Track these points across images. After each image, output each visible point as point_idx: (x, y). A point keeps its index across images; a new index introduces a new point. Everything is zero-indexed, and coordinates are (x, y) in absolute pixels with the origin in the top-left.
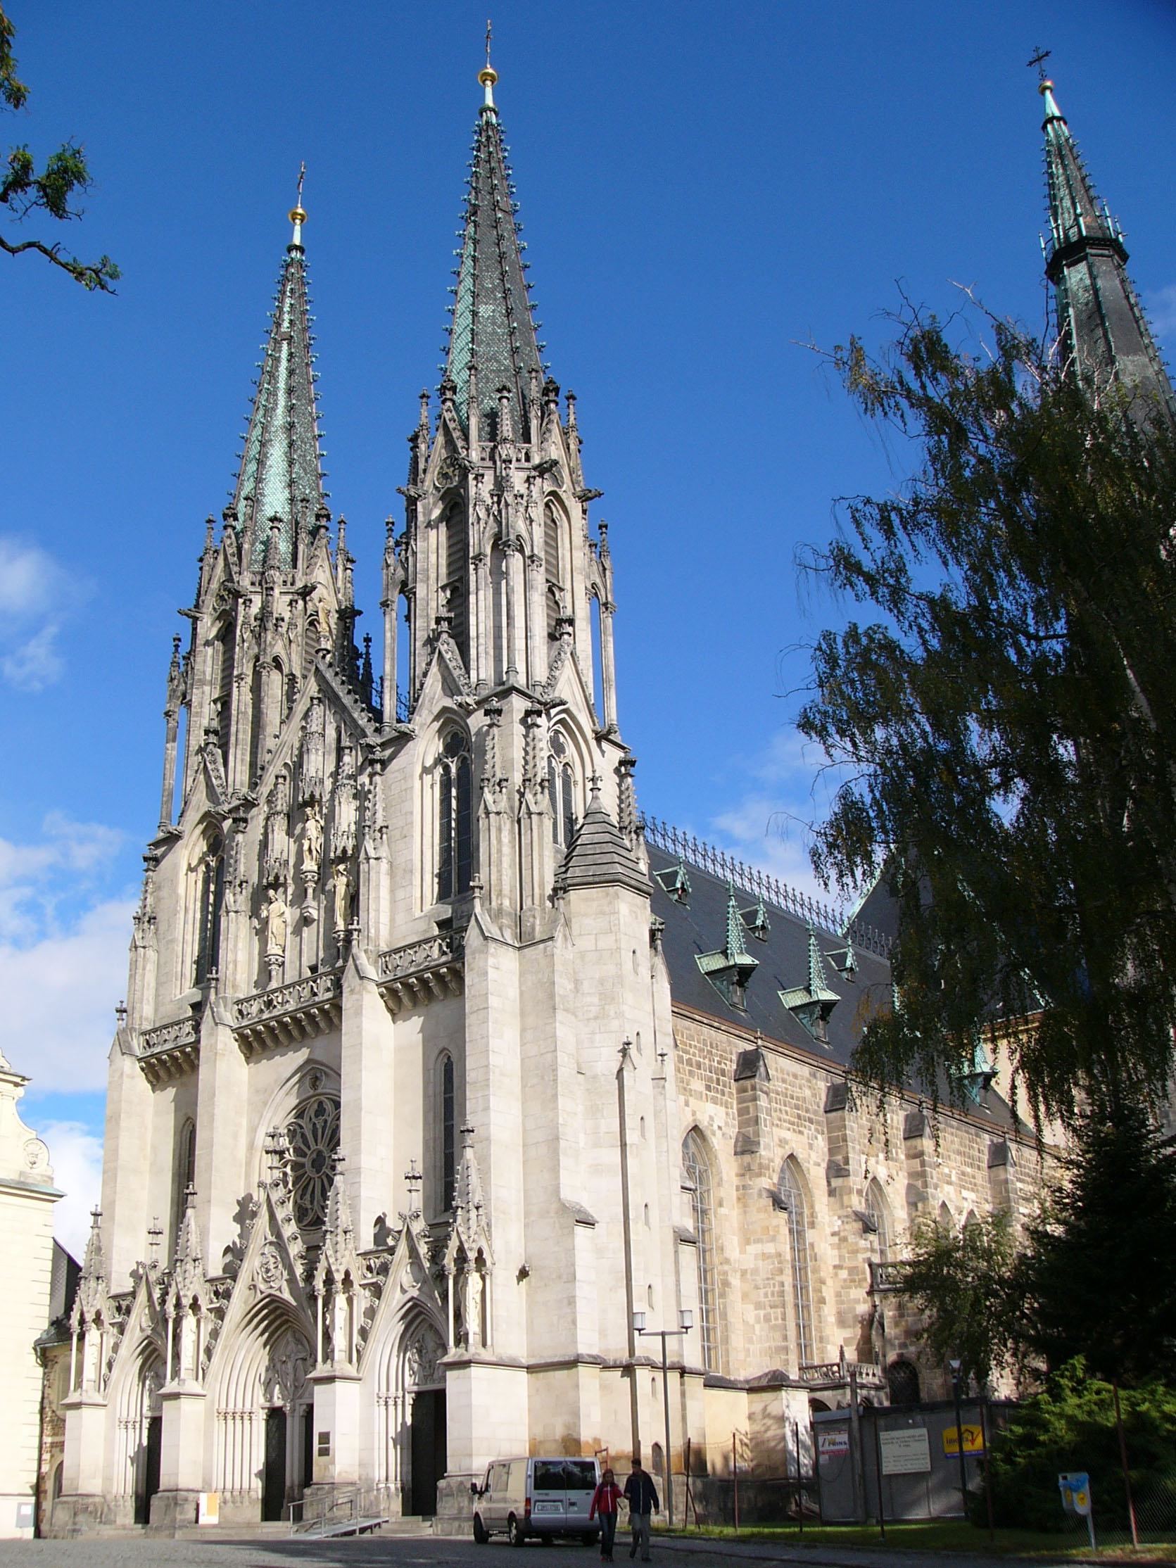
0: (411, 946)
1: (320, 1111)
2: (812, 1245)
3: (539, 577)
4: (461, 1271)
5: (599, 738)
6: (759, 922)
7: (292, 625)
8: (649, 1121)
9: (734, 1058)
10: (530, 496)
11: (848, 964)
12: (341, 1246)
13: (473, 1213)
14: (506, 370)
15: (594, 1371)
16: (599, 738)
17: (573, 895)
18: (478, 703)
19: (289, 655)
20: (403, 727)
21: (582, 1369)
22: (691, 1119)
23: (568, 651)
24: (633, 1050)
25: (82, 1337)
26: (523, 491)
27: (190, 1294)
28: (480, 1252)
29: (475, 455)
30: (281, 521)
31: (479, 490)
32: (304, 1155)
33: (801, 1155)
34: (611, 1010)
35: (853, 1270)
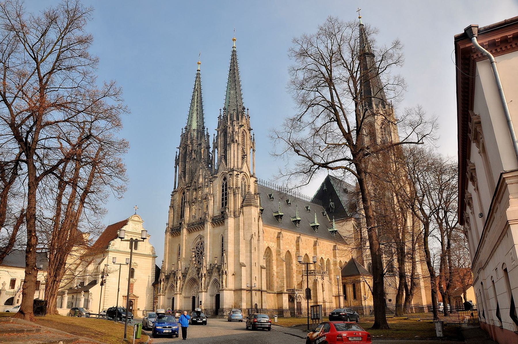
0: (216, 216)
1: (202, 244)
2: (292, 267)
3: (240, 148)
5: (251, 177)
6: (289, 203)
8: (257, 248)
9: (277, 233)
10: (239, 131)
11: (309, 209)
12: (204, 269)
13: (225, 265)
14: (236, 105)
15: (245, 291)
16: (251, 177)
17: (244, 208)
18: (228, 172)
19: (197, 157)
20: (215, 176)
21: (242, 291)
22: (267, 245)
24: (254, 236)
25: (160, 283)
26: (237, 131)
27: (179, 276)
28: (226, 271)
29: (229, 123)
31: (230, 130)
32: (199, 252)
33: (290, 250)
35: (300, 271)
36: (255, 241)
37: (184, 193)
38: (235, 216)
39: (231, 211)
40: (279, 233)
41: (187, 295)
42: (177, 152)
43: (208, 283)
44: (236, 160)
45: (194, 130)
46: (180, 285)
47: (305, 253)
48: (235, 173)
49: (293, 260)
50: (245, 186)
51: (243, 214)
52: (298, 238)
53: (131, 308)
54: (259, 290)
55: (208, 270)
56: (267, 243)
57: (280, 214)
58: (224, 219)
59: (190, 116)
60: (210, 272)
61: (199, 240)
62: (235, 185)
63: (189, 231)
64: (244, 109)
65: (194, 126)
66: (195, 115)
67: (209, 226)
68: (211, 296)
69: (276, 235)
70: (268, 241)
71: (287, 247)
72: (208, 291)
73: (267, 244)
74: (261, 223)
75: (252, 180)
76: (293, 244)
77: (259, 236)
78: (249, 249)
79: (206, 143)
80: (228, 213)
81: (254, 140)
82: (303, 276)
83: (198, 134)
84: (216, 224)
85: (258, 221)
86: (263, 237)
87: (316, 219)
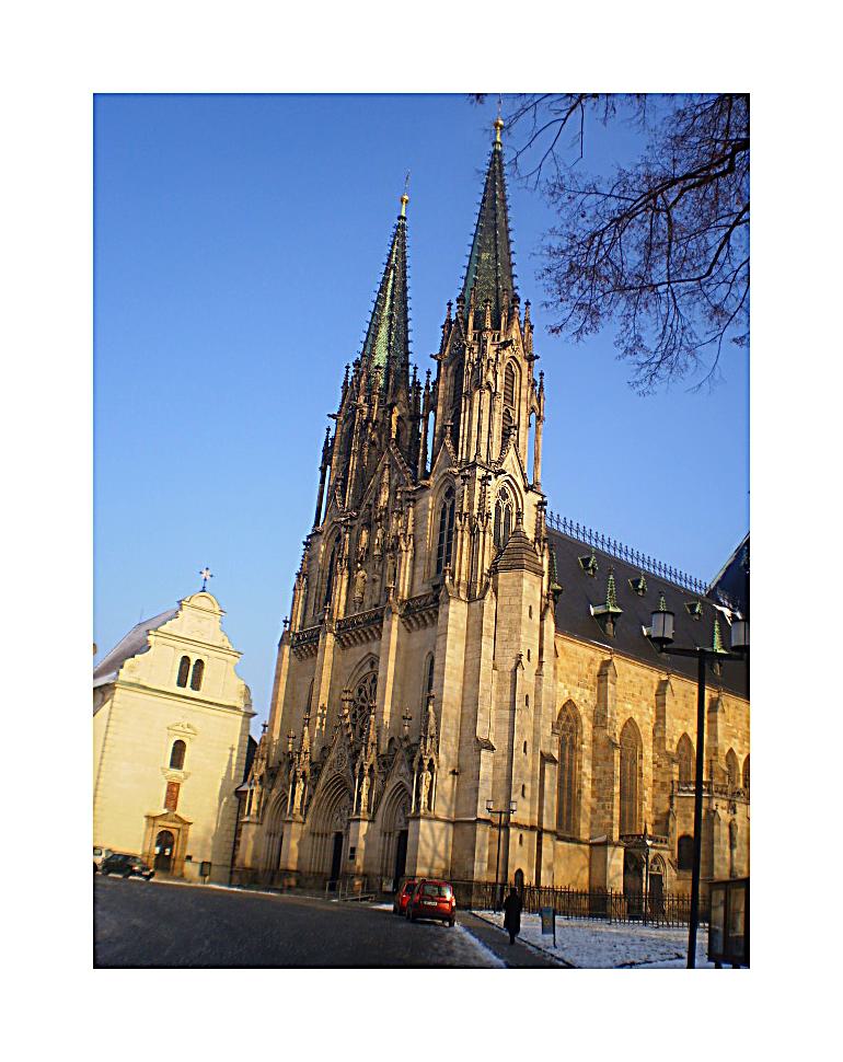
2: (641, 768)
3: (499, 403)
4: (421, 770)
5: (527, 490)
6: (640, 587)
7: (383, 424)
8: (531, 699)
9: (599, 664)
10: (497, 359)
16: (527, 490)
18: (460, 471)
19: (380, 440)
20: (423, 482)
23: (512, 443)
24: (524, 659)
28: (431, 761)
29: (470, 338)
30: (381, 368)
33: (636, 718)
34: (515, 637)
35: (663, 784)
36: (526, 676)
37: (338, 539)
38: (471, 599)
39: (459, 582)
40: (606, 664)
41: (320, 827)
42: (329, 430)
43: (380, 796)
44: (484, 439)
45: (378, 367)
46: (303, 796)
47: (681, 731)
48: (480, 473)
49: (645, 747)
50: (508, 514)
51: (496, 591)
52: (663, 684)
53: (167, 854)
54: (532, 828)
55: (383, 755)
56: (565, 687)
57: (611, 609)
58: (438, 606)
59: (372, 334)
60: (386, 762)
61: (367, 669)
62: (476, 506)
63: (343, 643)
64: (516, 299)
65: (381, 357)
66: (383, 331)
67: (394, 626)
68: (386, 833)
69: (596, 668)
70: (570, 681)
71: (630, 707)
72: (379, 819)
73: (566, 691)
74: (550, 624)
75: (531, 499)
76: (646, 700)
77: (541, 663)
78: (507, 697)
79: (410, 405)
80: (450, 587)
81: (541, 388)
82: (671, 798)
83: (387, 379)
84: (416, 619)
85: (542, 619)
86: (555, 668)
87: (717, 638)
